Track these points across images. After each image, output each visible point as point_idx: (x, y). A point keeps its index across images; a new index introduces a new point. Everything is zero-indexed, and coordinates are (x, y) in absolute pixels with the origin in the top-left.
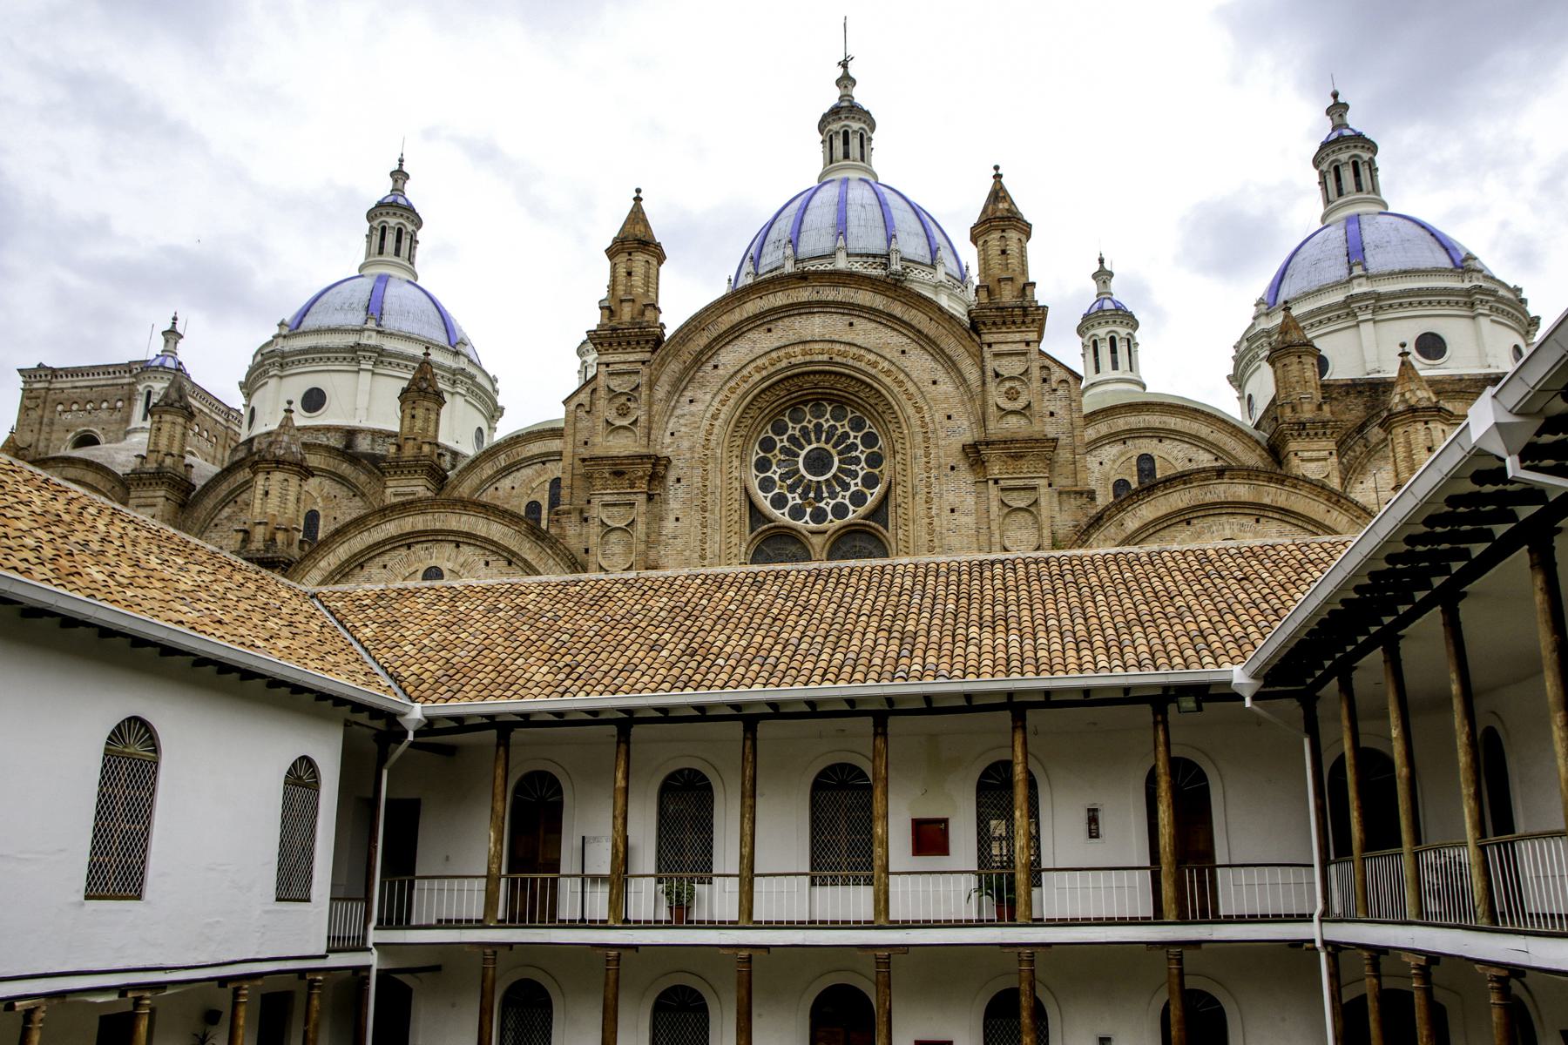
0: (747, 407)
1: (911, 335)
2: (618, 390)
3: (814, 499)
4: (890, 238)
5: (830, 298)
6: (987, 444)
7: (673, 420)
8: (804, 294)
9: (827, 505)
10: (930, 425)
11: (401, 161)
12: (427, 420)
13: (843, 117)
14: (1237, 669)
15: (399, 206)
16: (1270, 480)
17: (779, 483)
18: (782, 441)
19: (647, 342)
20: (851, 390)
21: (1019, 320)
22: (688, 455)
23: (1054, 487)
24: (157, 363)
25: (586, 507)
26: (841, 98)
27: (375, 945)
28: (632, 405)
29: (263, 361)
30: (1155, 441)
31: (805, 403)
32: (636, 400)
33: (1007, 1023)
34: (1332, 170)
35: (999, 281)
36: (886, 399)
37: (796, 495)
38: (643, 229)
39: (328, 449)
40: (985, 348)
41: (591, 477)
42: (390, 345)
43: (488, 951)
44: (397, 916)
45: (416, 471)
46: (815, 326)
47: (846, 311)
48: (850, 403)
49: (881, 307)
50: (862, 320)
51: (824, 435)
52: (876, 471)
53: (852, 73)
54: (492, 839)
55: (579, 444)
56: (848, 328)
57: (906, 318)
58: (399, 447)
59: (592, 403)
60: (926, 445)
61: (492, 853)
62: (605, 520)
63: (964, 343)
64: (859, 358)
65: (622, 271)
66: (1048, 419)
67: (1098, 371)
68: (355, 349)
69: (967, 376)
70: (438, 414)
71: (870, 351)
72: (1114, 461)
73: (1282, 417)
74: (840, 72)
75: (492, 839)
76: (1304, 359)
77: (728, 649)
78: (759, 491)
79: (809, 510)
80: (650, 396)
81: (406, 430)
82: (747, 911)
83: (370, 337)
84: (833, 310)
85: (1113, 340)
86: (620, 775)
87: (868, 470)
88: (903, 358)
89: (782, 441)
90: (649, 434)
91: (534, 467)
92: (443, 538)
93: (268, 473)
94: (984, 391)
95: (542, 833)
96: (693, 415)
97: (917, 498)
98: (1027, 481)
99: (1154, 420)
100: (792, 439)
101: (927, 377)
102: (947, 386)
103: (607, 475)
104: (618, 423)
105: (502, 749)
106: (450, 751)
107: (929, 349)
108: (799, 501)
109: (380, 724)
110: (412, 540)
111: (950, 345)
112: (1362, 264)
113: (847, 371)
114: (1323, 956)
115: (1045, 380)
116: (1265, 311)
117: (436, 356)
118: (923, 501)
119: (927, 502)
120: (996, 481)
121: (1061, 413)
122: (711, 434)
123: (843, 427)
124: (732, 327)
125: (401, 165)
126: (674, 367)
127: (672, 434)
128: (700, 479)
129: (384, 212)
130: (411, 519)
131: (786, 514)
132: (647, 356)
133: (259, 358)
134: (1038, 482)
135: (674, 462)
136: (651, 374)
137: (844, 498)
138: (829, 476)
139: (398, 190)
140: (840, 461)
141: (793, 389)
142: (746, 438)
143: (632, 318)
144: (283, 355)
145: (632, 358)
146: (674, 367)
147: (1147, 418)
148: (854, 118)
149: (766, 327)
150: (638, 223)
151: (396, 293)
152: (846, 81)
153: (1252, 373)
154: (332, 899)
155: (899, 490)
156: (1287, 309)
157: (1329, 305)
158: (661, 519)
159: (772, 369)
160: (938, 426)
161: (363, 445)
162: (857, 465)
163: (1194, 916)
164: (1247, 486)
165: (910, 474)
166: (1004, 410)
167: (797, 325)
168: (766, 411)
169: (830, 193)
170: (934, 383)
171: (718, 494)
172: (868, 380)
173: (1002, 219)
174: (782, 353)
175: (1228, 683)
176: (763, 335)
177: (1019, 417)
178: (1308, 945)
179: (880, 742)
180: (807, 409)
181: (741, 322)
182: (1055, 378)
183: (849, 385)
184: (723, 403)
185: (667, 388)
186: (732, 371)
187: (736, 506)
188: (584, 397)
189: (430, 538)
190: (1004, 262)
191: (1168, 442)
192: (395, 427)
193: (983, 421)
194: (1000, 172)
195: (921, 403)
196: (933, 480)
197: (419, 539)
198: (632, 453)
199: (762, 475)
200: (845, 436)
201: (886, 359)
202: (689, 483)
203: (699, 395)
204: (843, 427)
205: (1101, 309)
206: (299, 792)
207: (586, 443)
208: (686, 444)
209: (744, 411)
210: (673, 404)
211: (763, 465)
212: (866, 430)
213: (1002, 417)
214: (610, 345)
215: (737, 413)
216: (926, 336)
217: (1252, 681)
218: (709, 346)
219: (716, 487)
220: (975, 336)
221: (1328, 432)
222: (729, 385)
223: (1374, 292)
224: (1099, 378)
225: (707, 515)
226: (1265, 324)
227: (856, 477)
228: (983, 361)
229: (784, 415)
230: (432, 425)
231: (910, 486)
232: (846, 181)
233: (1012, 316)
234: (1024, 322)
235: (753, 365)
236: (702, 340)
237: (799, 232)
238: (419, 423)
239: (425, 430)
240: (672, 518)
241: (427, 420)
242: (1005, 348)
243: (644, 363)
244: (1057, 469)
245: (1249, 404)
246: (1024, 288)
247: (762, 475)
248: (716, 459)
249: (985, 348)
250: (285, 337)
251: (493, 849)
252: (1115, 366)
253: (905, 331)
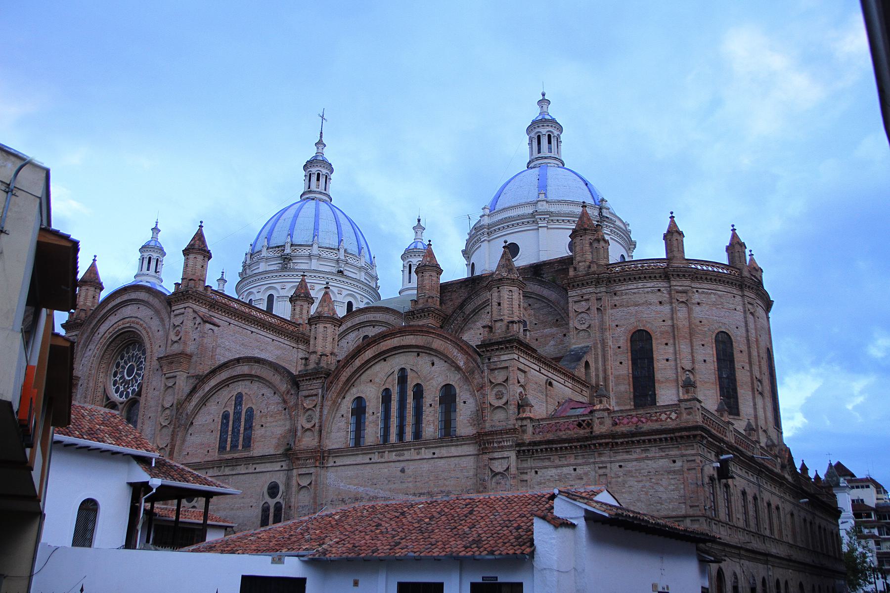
40: (172, 313)
101: (156, 329)
125: (157, 225)
147: (368, 315)
149: (114, 314)
152: (320, 143)
187: (99, 394)
209: (105, 352)
221: (426, 314)
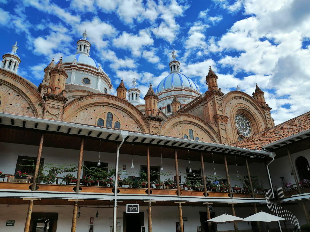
93: (154, 99)
110: (186, 122)
145: (220, 98)
189: (189, 123)
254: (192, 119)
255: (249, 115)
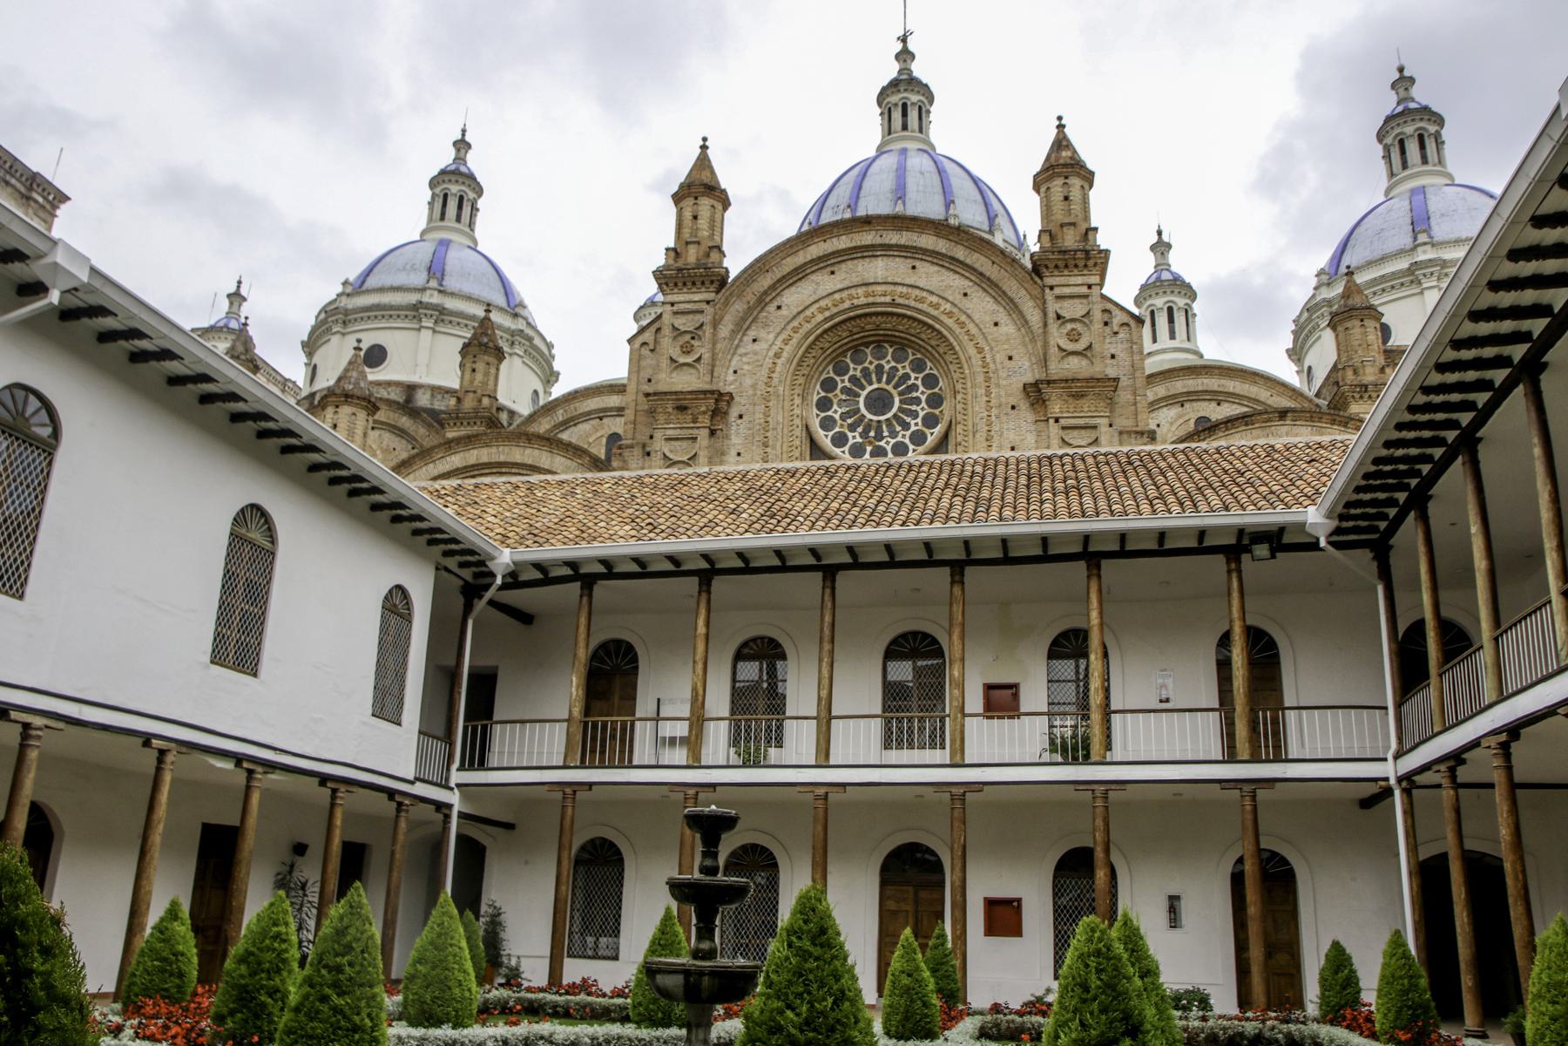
0: (810, 347)
1: (973, 278)
2: (682, 328)
3: (875, 438)
4: (949, 203)
5: (893, 242)
6: (1049, 382)
7: (736, 358)
8: (868, 238)
9: (887, 443)
10: (992, 366)
11: (464, 131)
12: (487, 374)
13: (902, 89)
14: (1311, 509)
15: (461, 174)
16: (1333, 422)
17: (839, 422)
18: (843, 382)
19: (712, 282)
20: (912, 331)
21: (1081, 263)
22: (751, 392)
23: (1114, 427)
24: (221, 324)
25: (648, 441)
26: (900, 72)
27: (458, 785)
28: (695, 343)
29: (326, 319)
30: (1214, 404)
31: (867, 345)
32: (700, 338)
33: (1077, 883)
34: (1396, 143)
35: (1062, 226)
36: (947, 340)
37: (857, 434)
38: (709, 175)
39: (390, 403)
40: (1047, 291)
41: (655, 412)
42: (451, 304)
43: (568, 790)
44: (477, 757)
45: (475, 423)
46: (878, 269)
47: (909, 255)
48: (911, 344)
49: (944, 251)
50: (927, 264)
51: (885, 376)
52: (937, 412)
53: (911, 46)
54: (574, 684)
55: (642, 381)
56: (911, 271)
57: (968, 261)
58: (459, 400)
59: (655, 341)
60: (987, 384)
61: (574, 697)
62: (668, 454)
63: (1026, 285)
64: (922, 300)
65: (688, 214)
66: (1109, 361)
67: (1155, 341)
68: (417, 307)
69: (1029, 317)
70: (498, 369)
71: (932, 293)
72: (1171, 424)
73: (1343, 380)
74: (899, 46)
75: (574, 684)
76: (1366, 322)
77: (807, 511)
78: (820, 430)
79: (869, 449)
80: (714, 334)
81: (466, 383)
82: (824, 750)
83: (432, 295)
84: (896, 253)
85: (1170, 310)
86: (701, 622)
87: (928, 410)
88: (964, 300)
89: (843, 382)
90: (712, 372)
91: (591, 422)
92: (507, 470)
93: (337, 407)
94: (1045, 333)
95: (616, 700)
96: (756, 353)
97: (978, 436)
98: (1087, 420)
99: (1212, 383)
100: (853, 379)
101: (989, 319)
102: (1008, 328)
103: (670, 410)
104: (682, 360)
105: (585, 599)
106: (525, 618)
107: (991, 291)
108: (859, 440)
109: (467, 574)
111: (1012, 287)
112: (1428, 231)
113: (909, 313)
114: (1397, 793)
115: (1106, 324)
116: (1326, 282)
117: (495, 317)
118: (983, 439)
119: (987, 440)
120: (1057, 420)
121: (1122, 355)
122: (773, 372)
123: (904, 368)
124: (796, 269)
125: (463, 135)
126: (738, 307)
127: (735, 372)
128: (761, 416)
129: (446, 179)
130: (475, 452)
131: (847, 452)
132: (711, 296)
133: (323, 316)
134: (1098, 421)
135: (737, 399)
136: (716, 314)
137: (904, 437)
138: (889, 415)
139: (460, 159)
140: (901, 401)
141: (855, 330)
142: (808, 377)
143: (698, 259)
144: (346, 312)
145: (697, 297)
146: (738, 307)
148: (912, 90)
149: (829, 269)
150: (704, 169)
151: (457, 257)
153: (1311, 346)
154: (420, 732)
155: (960, 429)
156: (1350, 274)
157: (1393, 273)
158: (723, 454)
159: (835, 310)
160: (999, 366)
161: (423, 400)
162: (918, 405)
163: (1267, 753)
164: (1310, 428)
165: (970, 413)
166: (1065, 351)
167: (860, 268)
168: (828, 352)
169: (889, 161)
170: (996, 324)
171: (779, 430)
172: (930, 322)
173: (1065, 165)
174: (845, 294)
175: (1303, 525)
176: (826, 277)
177: (1080, 357)
178: (1383, 783)
179: (957, 590)
180: (868, 351)
181: (805, 264)
182: (1116, 322)
183: (910, 327)
184: (786, 342)
185: (731, 327)
186: (795, 311)
187: (797, 442)
188: (648, 336)
189: (494, 470)
190: (1067, 208)
191: (1226, 405)
192: (455, 384)
193: (1044, 361)
194: (1063, 122)
195: (982, 344)
196: (993, 418)
197: (483, 471)
198: (695, 389)
199: (823, 415)
200: (906, 377)
201: (947, 301)
202: (751, 419)
203: (762, 334)
204: (904, 368)
205: (1158, 279)
206: (394, 620)
207: (650, 380)
208: (748, 381)
209: (806, 351)
210: (736, 342)
211: (824, 404)
212: (927, 372)
213: (1063, 358)
214: (676, 285)
215: (800, 353)
216: (989, 279)
217: (1327, 521)
218: (773, 287)
219: (778, 424)
220: (1037, 279)
222: (792, 325)
223: (1440, 259)
224: (1156, 347)
225: (768, 450)
226: (1327, 294)
227: (916, 417)
228: (1045, 303)
229: (845, 357)
230: (492, 379)
231: (970, 424)
232: (904, 151)
233: (1075, 259)
234: (1086, 266)
235: (816, 306)
236: (766, 281)
237: (858, 197)
238: (479, 377)
239: (485, 384)
240: (733, 453)
241: (487, 374)
242: (1067, 291)
243: (708, 302)
244: (1117, 410)
245: (1308, 376)
246: (1086, 233)
247: (823, 415)
248: (778, 396)
249: (1047, 291)
250: (348, 295)
251: (574, 694)
252: (1172, 336)
253: (967, 274)
254: (506, 449)
255: (923, 336)
